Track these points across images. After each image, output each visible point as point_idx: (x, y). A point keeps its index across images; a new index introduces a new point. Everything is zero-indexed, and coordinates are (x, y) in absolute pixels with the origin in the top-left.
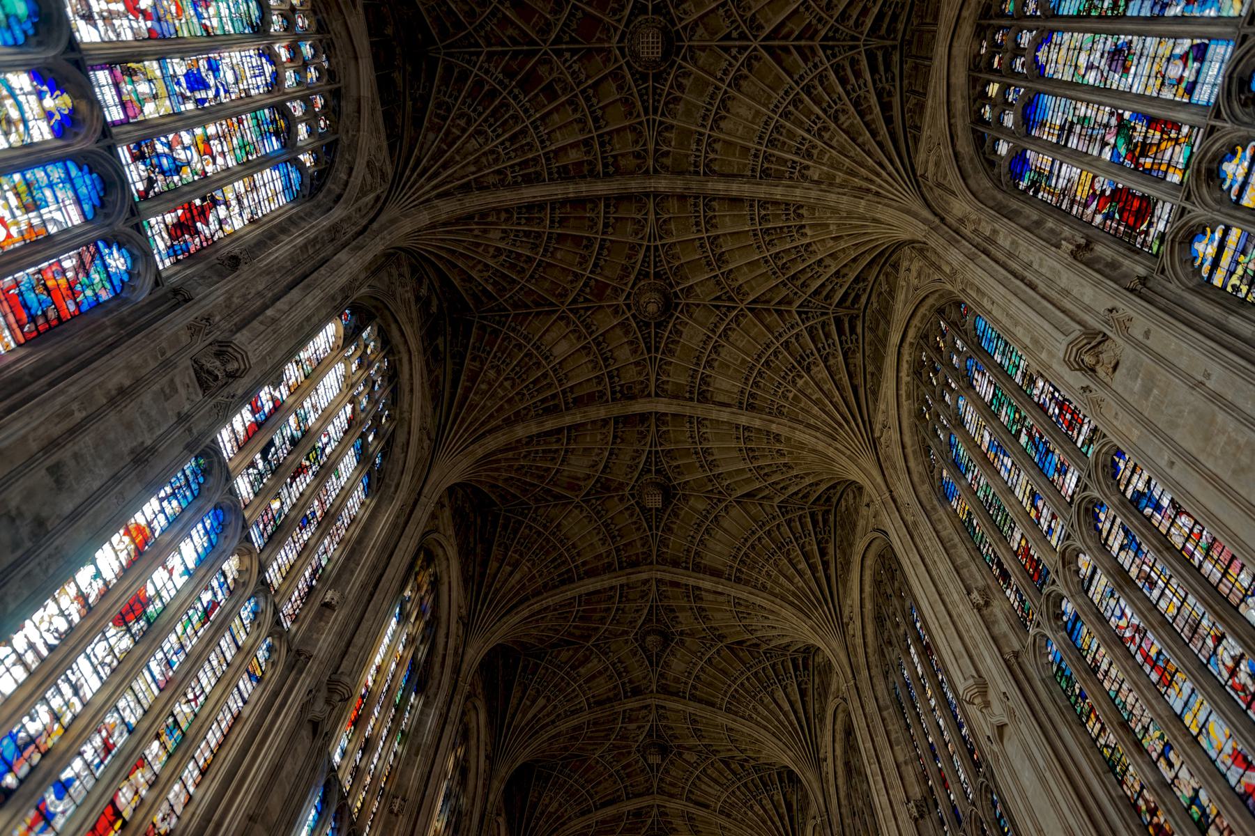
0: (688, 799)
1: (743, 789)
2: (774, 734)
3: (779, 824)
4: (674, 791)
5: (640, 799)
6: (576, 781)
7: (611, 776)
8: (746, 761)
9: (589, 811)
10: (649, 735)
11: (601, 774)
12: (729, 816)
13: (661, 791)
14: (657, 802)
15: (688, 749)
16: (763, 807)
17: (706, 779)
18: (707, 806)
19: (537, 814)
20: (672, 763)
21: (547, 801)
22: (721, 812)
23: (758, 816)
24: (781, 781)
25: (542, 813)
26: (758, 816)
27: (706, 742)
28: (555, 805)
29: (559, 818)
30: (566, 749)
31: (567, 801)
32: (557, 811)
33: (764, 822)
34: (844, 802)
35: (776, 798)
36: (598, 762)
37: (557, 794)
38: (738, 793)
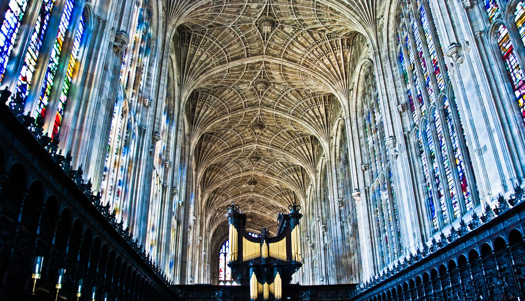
0: (284, 58)
1: (319, 50)
2: (348, 6)
3: (338, 69)
4: (276, 52)
5: (255, 57)
6: (217, 42)
7: (239, 40)
8: (324, 31)
9: (225, 62)
10: (264, 14)
11: (233, 39)
12: (308, 66)
13: (268, 53)
14: (266, 59)
15: (286, 24)
16: (330, 60)
17: (297, 44)
18: (295, 62)
19: (194, 61)
20: (277, 34)
21: (200, 53)
22: (304, 65)
23: (326, 65)
24: (343, 45)
25: (197, 61)
26: (326, 65)
27: (301, 17)
28: (204, 56)
29: (207, 65)
30: (212, 18)
31: (212, 55)
32: (206, 60)
33: (329, 69)
34: (391, 39)
35: (338, 55)
36: (231, 31)
37: (205, 49)
38: (315, 52)
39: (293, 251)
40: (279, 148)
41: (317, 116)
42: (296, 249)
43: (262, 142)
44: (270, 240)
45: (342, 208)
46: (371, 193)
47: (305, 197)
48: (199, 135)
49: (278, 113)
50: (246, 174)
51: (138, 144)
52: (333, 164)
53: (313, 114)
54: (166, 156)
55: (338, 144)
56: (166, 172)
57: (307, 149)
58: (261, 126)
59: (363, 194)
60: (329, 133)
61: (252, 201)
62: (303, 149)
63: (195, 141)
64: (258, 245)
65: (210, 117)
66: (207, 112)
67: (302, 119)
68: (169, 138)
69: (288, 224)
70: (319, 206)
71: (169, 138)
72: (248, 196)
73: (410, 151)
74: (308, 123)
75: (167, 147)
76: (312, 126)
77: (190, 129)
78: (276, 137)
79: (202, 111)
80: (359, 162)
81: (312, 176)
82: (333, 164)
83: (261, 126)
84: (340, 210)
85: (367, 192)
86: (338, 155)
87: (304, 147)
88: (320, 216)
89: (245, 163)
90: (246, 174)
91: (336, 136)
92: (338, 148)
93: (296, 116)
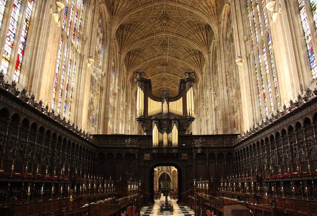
39: (188, 108)
40: (182, 35)
41: (209, 7)
42: (190, 106)
43: (169, 32)
44: (170, 99)
45: (228, 76)
46: (251, 59)
47: (202, 73)
48: (119, 23)
49: (179, 6)
50: (159, 58)
51: (41, 7)
52: (222, 43)
53: (206, 5)
54: (84, 32)
55: (225, 27)
56: (83, 44)
57: (202, 36)
58: (168, 18)
59: (244, 60)
60: (218, 19)
61: (164, 79)
62: (199, 36)
63: (115, 27)
64: (160, 103)
65: (126, 9)
66: (124, 5)
67: (198, 9)
68: (86, 17)
69: (185, 87)
70: (212, 78)
71: (86, 17)
72: (162, 75)
73: (289, 9)
74: (202, 12)
75: (85, 25)
76: (205, 15)
77: (111, 19)
78: (179, 27)
79: (120, 4)
80: (242, 34)
81: (206, 56)
82: (222, 43)
83: (168, 18)
84: (226, 78)
85: (248, 58)
86: (225, 36)
87: (200, 34)
88: (212, 85)
89: (157, 49)
90: (159, 58)
91: (224, 21)
92: (225, 30)
93: (193, 7)
